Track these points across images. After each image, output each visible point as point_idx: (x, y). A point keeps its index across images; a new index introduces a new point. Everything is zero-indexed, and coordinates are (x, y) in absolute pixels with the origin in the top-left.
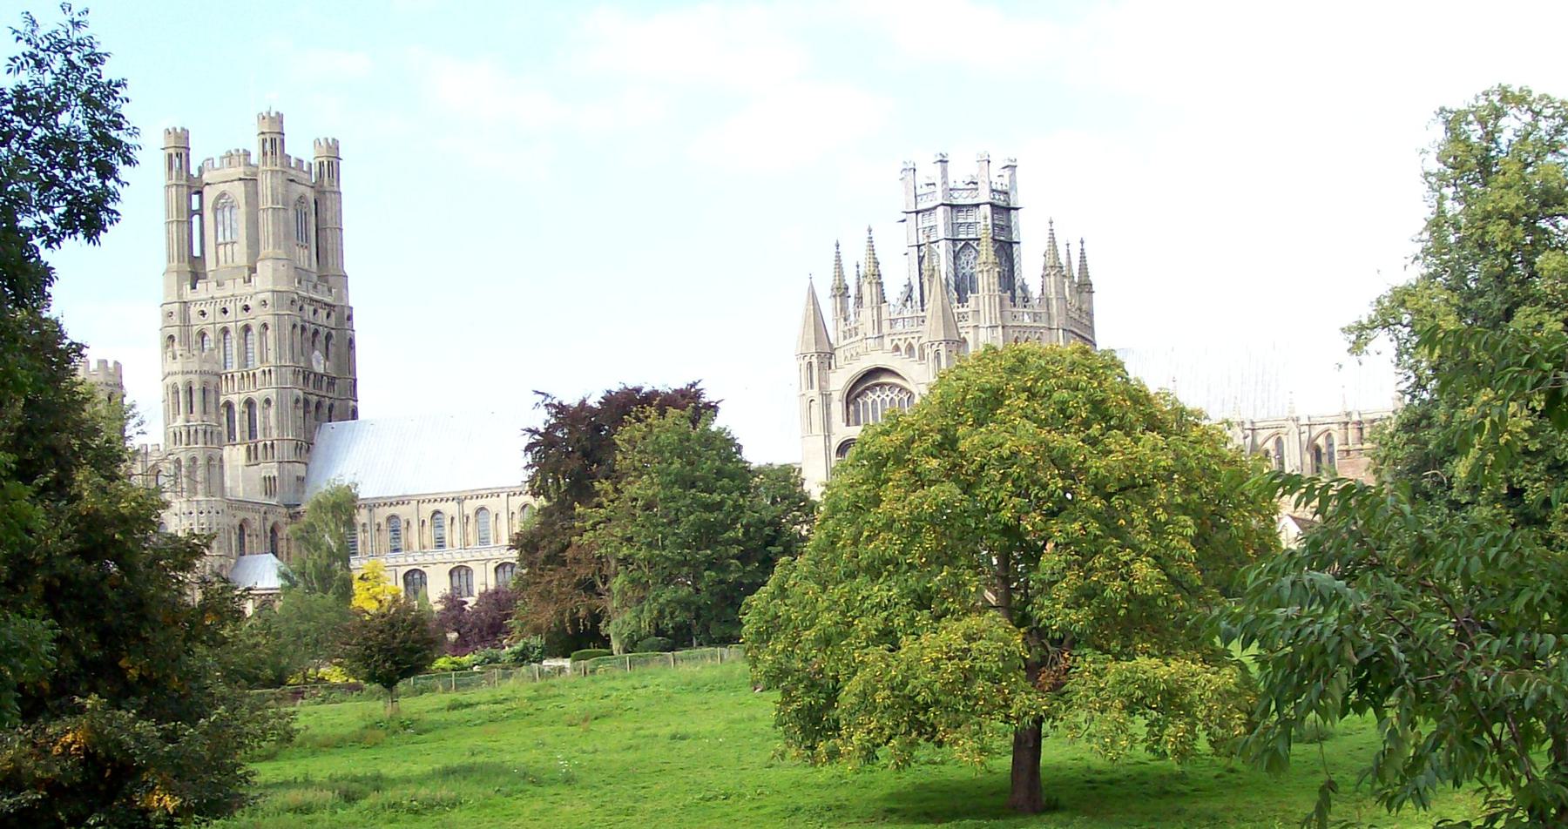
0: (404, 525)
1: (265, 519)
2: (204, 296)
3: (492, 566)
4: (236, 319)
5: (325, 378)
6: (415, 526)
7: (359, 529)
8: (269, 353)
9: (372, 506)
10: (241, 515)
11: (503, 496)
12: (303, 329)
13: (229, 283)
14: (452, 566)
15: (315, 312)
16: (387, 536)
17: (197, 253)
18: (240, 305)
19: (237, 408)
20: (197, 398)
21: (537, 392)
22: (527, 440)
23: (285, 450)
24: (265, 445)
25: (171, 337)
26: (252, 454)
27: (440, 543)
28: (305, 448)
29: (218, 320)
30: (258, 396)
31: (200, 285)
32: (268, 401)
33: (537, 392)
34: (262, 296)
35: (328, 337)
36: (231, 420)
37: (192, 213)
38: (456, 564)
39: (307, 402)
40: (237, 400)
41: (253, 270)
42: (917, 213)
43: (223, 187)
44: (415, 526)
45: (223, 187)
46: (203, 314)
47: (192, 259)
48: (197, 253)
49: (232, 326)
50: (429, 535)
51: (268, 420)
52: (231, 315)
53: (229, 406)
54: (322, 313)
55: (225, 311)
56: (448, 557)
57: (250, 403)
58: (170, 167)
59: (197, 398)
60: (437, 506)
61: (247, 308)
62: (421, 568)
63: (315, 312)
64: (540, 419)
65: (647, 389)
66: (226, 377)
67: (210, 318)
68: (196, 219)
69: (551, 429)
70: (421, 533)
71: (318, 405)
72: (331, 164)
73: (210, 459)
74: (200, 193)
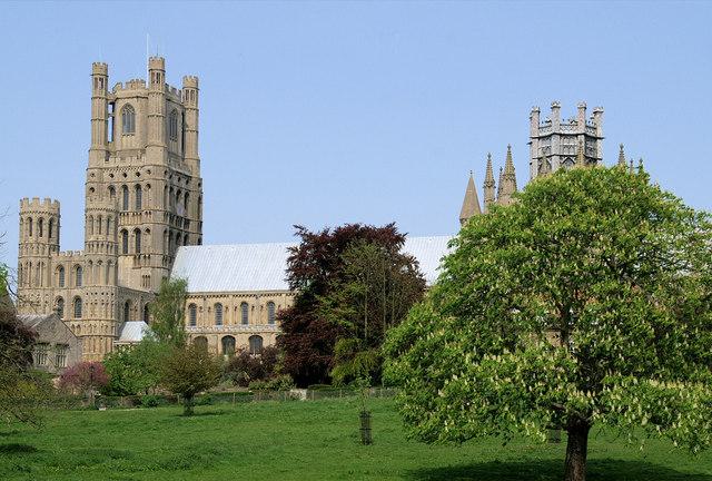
0: (224, 309)
3: (274, 336)
4: (132, 179)
6: (231, 309)
7: (198, 310)
8: (154, 200)
9: (204, 296)
10: (126, 297)
11: (284, 295)
12: (171, 189)
13: (128, 159)
15: (179, 179)
16: (213, 315)
17: (110, 139)
18: (134, 173)
19: (130, 234)
20: (104, 224)
21: (296, 227)
22: (289, 254)
23: (157, 261)
25: (92, 189)
26: (137, 258)
27: (245, 321)
28: (169, 260)
30: (143, 228)
32: (148, 230)
33: (296, 227)
34: (147, 168)
35: (187, 195)
36: (125, 240)
37: (107, 115)
39: (171, 233)
41: (143, 151)
42: (539, 138)
43: (127, 101)
44: (231, 309)
45: (127, 101)
46: (112, 176)
47: (107, 143)
48: (110, 139)
50: (239, 315)
51: (147, 240)
52: (129, 178)
53: (125, 232)
54: (183, 181)
55: (125, 175)
56: (249, 330)
57: (138, 231)
58: (96, 86)
59: (104, 224)
60: (244, 299)
61: (138, 174)
63: (179, 179)
64: (297, 242)
65: (362, 226)
67: (116, 179)
68: (110, 119)
69: (304, 248)
70: (234, 315)
71: (179, 235)
72: (193, 91)
73: (110, 262)
74: (113, 104)
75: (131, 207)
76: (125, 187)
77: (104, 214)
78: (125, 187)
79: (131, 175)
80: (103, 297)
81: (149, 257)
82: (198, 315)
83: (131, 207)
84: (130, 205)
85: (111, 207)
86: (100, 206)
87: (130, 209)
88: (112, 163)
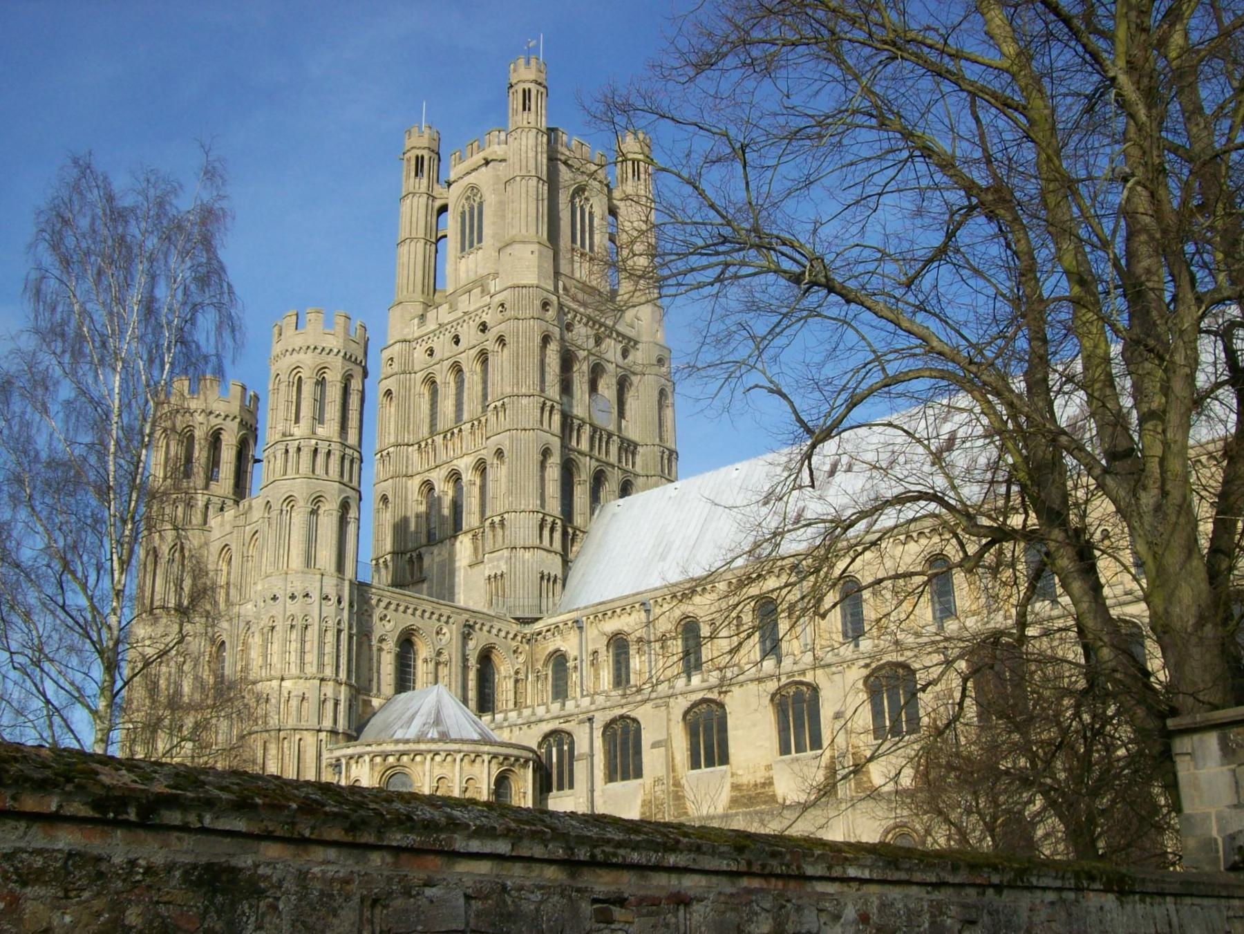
1: (466, 637)
2: (433, 327)
5: (615, 438)
14: (772, 686)
24: (493, 523)
29: (447, 355)
31: (431, 315)
38: (784, 680)
40: (465, 465)
49: (463, 359)
52: (463, 345)
55: (457, 340)
57: (481, 467)
59: (308, 389)
61: (484, 327)
62: (714, 695)
66: (453, 434)
75: (471, 408)
76: (457, 369)
77: (308, 361)
78: (457, 369)
79: (469, 334)
80: (294, 608)
81: (502, 522)
82: (636, 663)
83: (471, 408)
84: (465, 407)
85: (334, 342)
86: (299, 341)
87: (466, 417)
88: (431, 325)
